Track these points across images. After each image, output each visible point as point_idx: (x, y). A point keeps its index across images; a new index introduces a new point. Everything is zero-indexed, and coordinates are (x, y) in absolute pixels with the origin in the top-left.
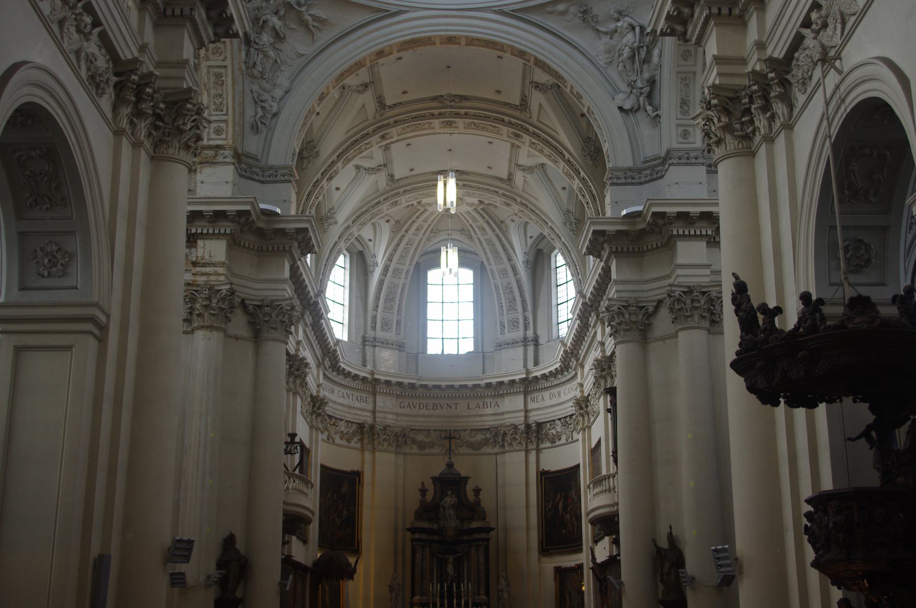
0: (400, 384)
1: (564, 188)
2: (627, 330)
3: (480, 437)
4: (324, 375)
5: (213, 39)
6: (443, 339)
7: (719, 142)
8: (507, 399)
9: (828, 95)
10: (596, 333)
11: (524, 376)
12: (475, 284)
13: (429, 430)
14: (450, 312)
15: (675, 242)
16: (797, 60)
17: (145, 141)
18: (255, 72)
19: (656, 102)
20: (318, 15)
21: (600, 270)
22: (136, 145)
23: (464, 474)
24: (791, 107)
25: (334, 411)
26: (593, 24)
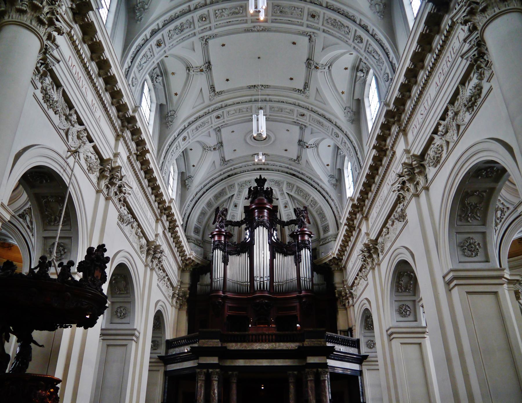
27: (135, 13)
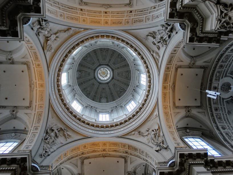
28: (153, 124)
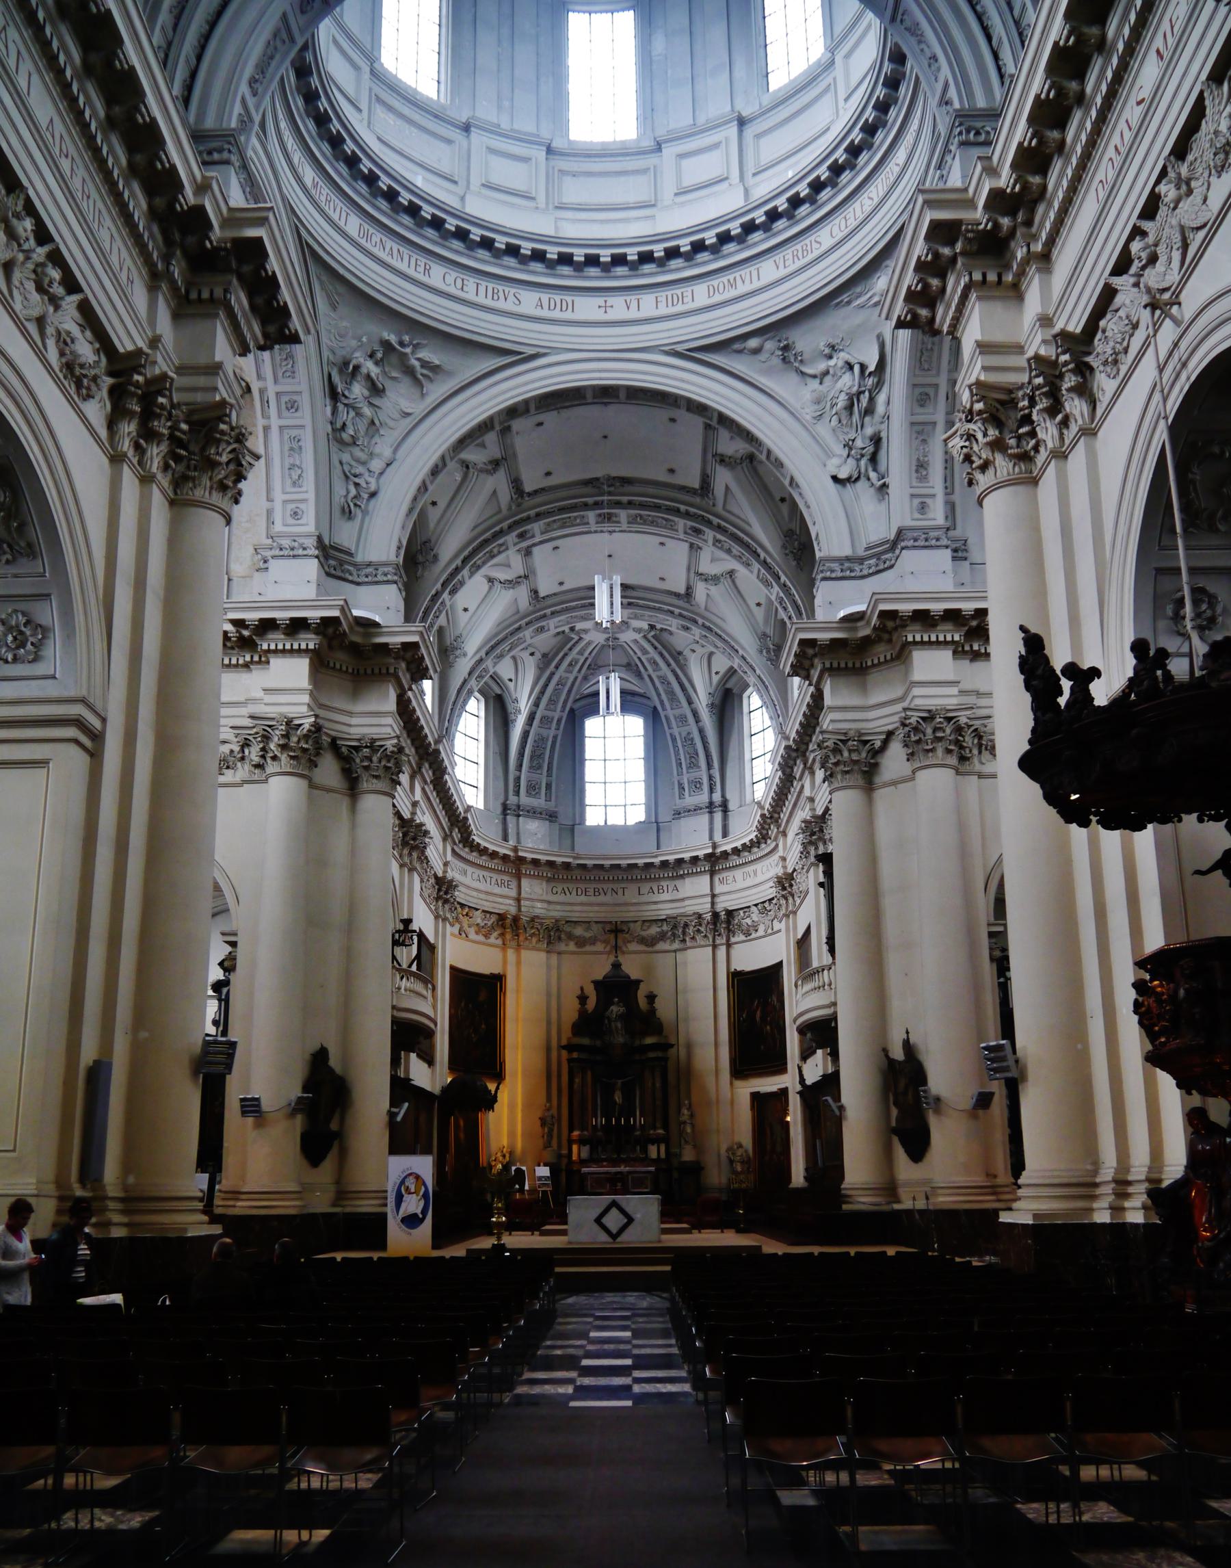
0: (551, 864)
1: (759, 604)
2: (847, 772)
3: (654, 930)
4: (453, 850)
5: (262, 342)
6: (606, 806)
7: (984, 467)
8: (688, 881)
9: (1163, 355)
10: (803, 787)
11: (710, 851)
12: (646, 736)
13: (589, 922)
14: (615, 772)
15: (910, 652)
16: (1104, 331)
17: (159, 476)
18: (344, 436)
19: (882, 467)
20: (428, 359)
21: (808, 699)
22: (146, 480)
23: (634, 976)
24: (1093, 403)
25: (468, 898)
26: (796, 364)
27: (447, 657)
28: (859, 326)
